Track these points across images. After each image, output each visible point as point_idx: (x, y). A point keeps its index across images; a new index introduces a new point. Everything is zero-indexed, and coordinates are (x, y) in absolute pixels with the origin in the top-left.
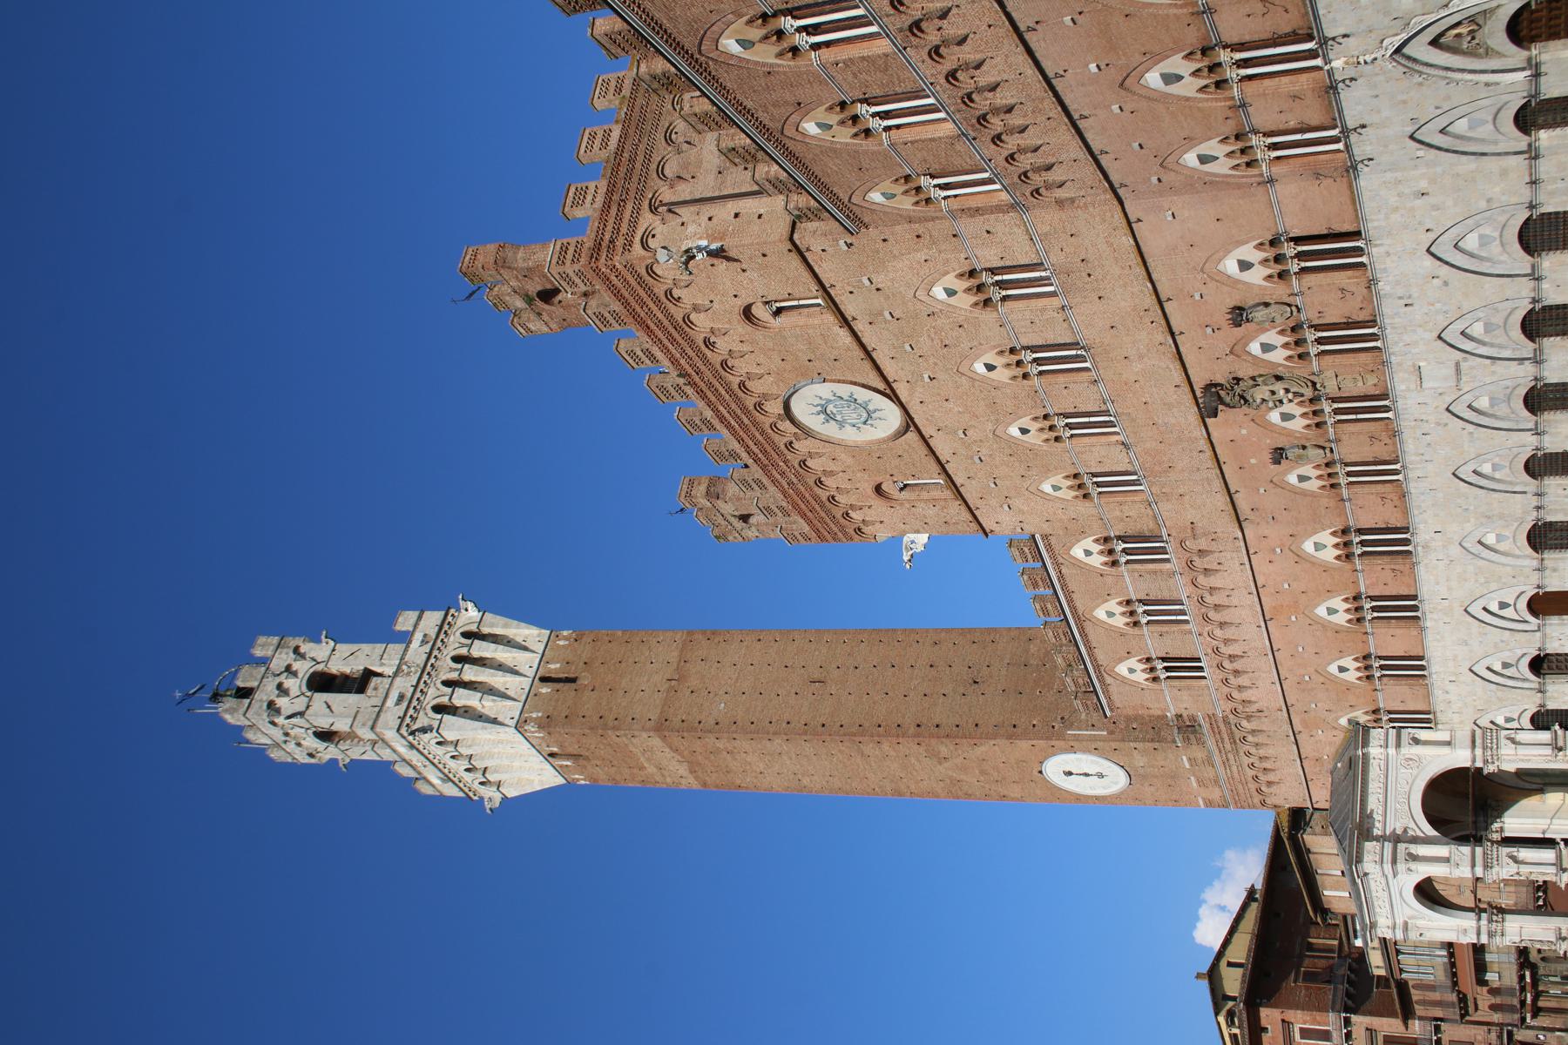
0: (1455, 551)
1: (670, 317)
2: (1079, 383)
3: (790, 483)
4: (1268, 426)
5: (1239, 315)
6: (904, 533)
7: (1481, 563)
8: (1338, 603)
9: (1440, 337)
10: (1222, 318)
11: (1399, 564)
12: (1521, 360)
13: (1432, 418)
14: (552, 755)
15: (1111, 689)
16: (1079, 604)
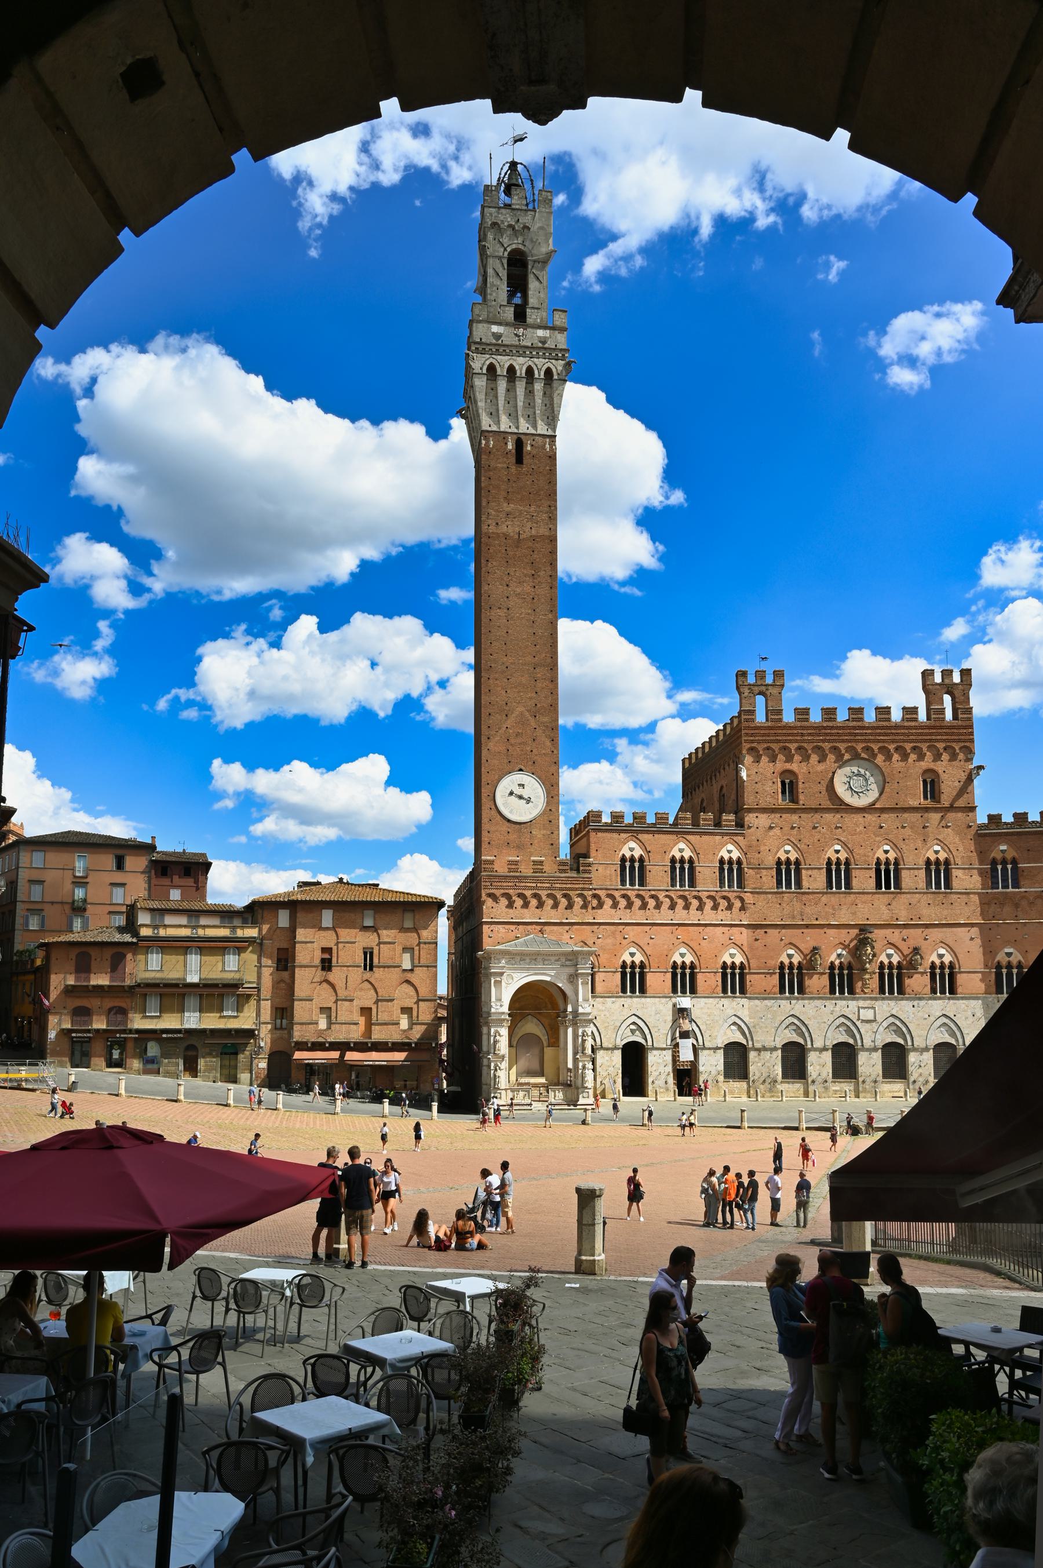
0: (731, 1012)
1: (938, 741)
2: (873, 882)
3: (802, 735)
4: (836, 947)
5: (916, 950)
6: (748, 770)
7: (721, 1022)
8: (689, 959)
9: (892, 1015)
10: (912, 943)
11: (720, 988)
12: (873, 1041)
13: (837, 1008)
14: (519, 444)
15: (615, 835)
16: (689, 837)
